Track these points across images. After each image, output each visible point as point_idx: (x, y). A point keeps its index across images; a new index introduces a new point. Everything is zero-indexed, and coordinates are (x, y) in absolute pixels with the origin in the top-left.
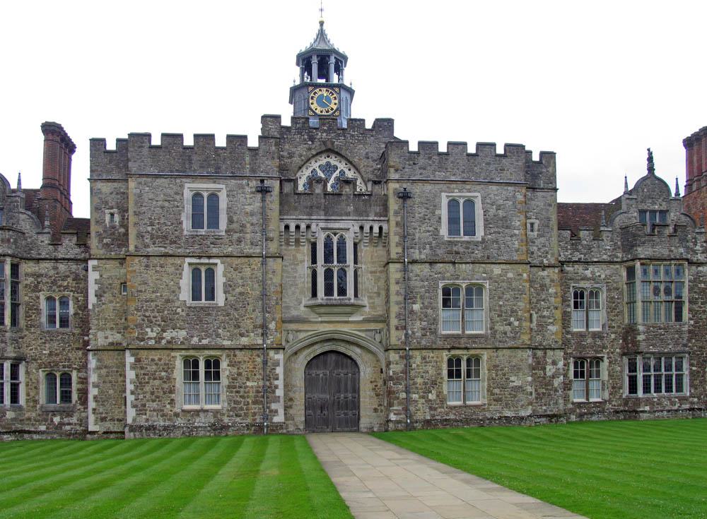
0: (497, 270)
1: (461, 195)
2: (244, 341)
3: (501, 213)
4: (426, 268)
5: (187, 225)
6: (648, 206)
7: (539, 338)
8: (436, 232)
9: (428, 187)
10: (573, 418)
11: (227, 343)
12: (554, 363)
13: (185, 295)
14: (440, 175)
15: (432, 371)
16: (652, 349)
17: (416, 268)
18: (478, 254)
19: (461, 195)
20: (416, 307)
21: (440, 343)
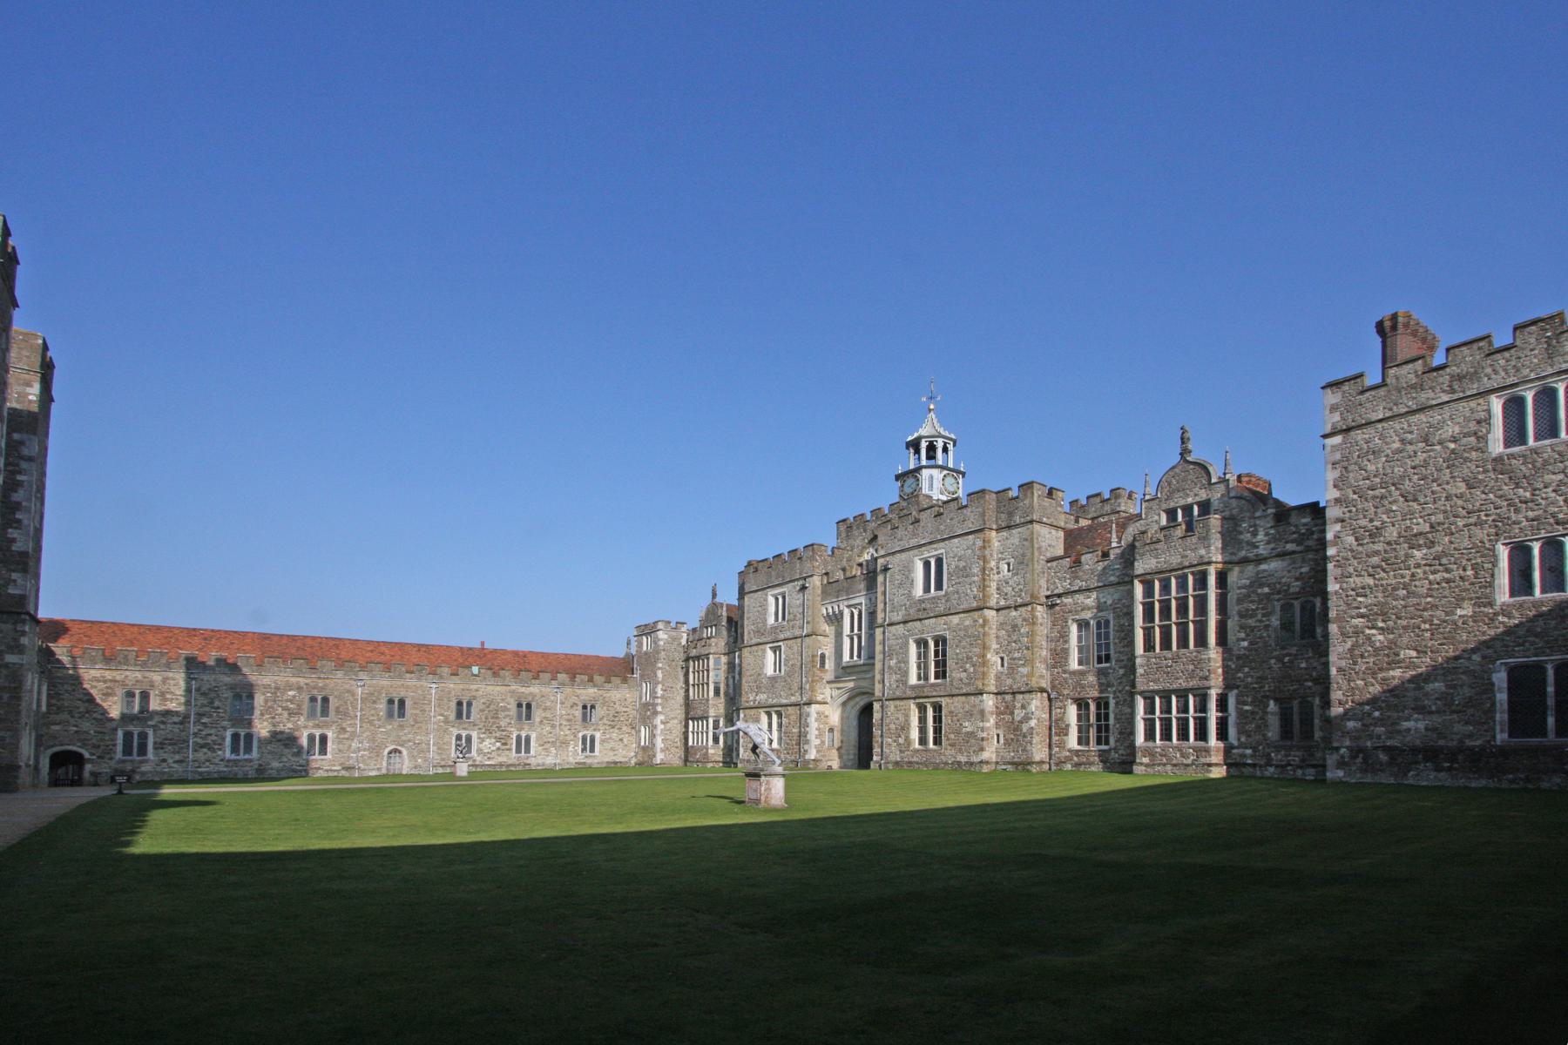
0: (955, 619)
1: (931, 553)
2: (793, 699)
3: (962, 564)
4: (900, 629)
5: (771, 620)
6: (1179, 501)
7: (1009, 682)
8: (909, 595)
9: (904, 556)
10: (1069, 767)
11: (784, 701)
12: (1023, 707)
13: (770, 670)
14: (914, 542)
15: (902, 719)
16: (1152, 686)
17: (893, 629)
18: (941, 608)
19: (931, 553)
20: (893, 663)
21: (909, 693)
